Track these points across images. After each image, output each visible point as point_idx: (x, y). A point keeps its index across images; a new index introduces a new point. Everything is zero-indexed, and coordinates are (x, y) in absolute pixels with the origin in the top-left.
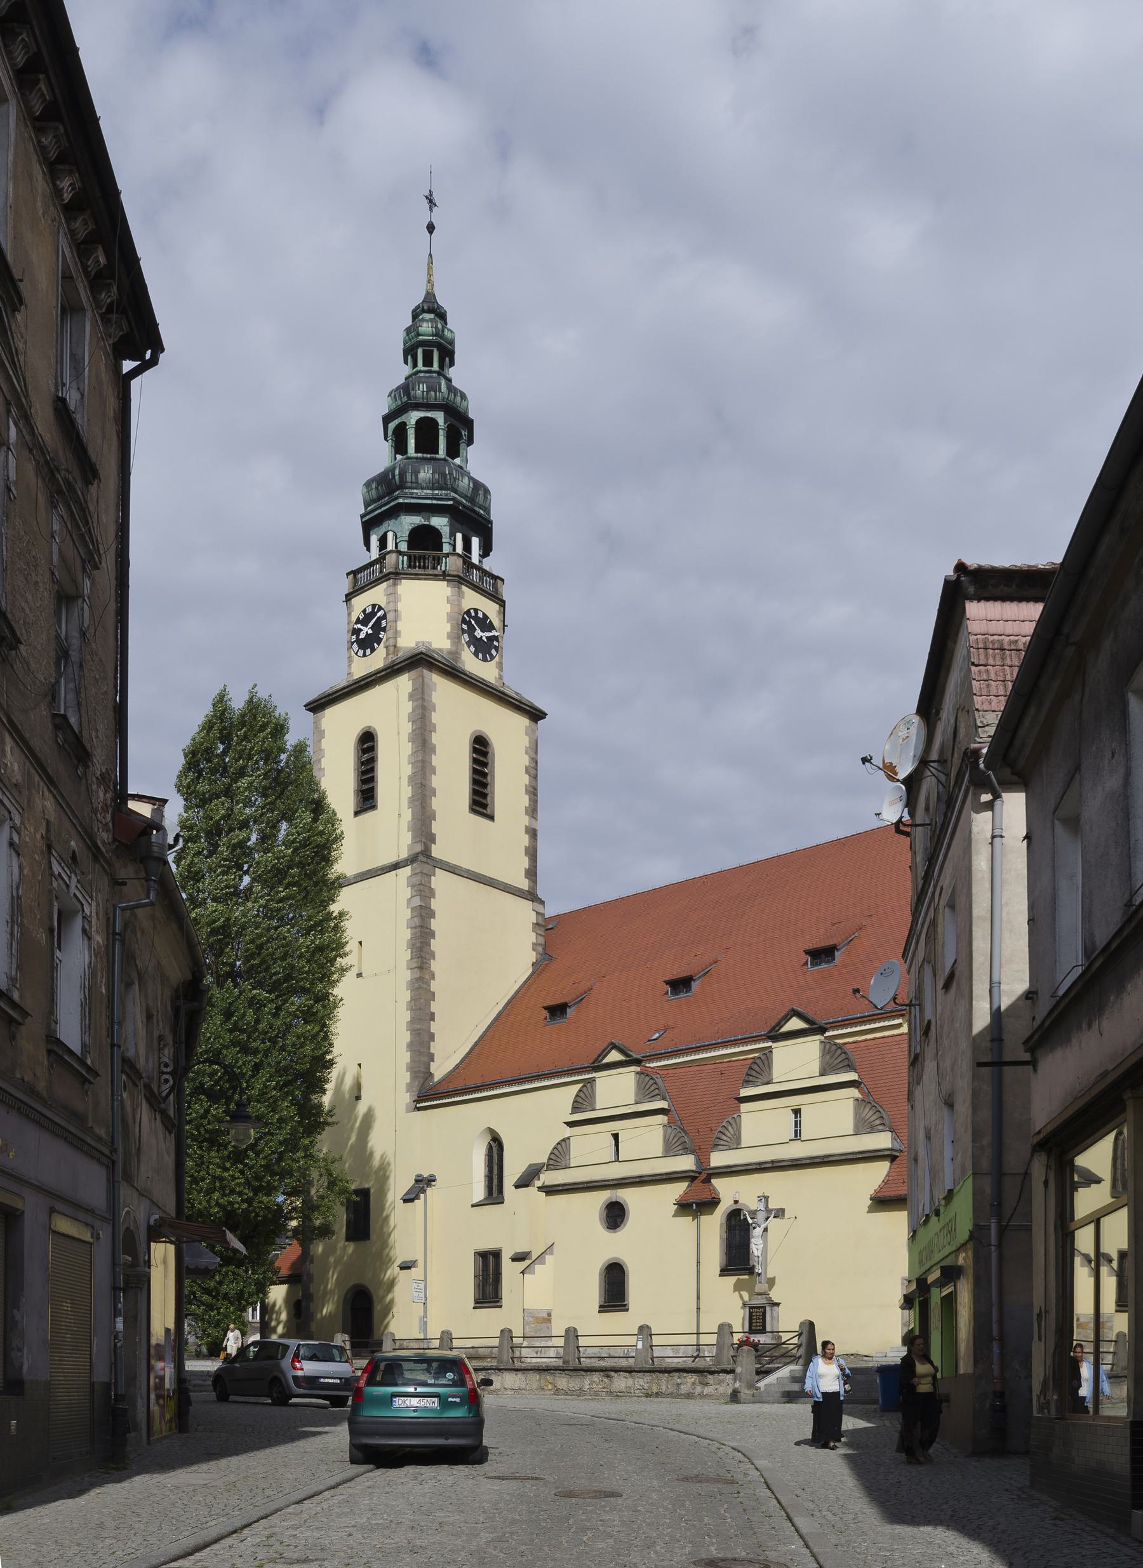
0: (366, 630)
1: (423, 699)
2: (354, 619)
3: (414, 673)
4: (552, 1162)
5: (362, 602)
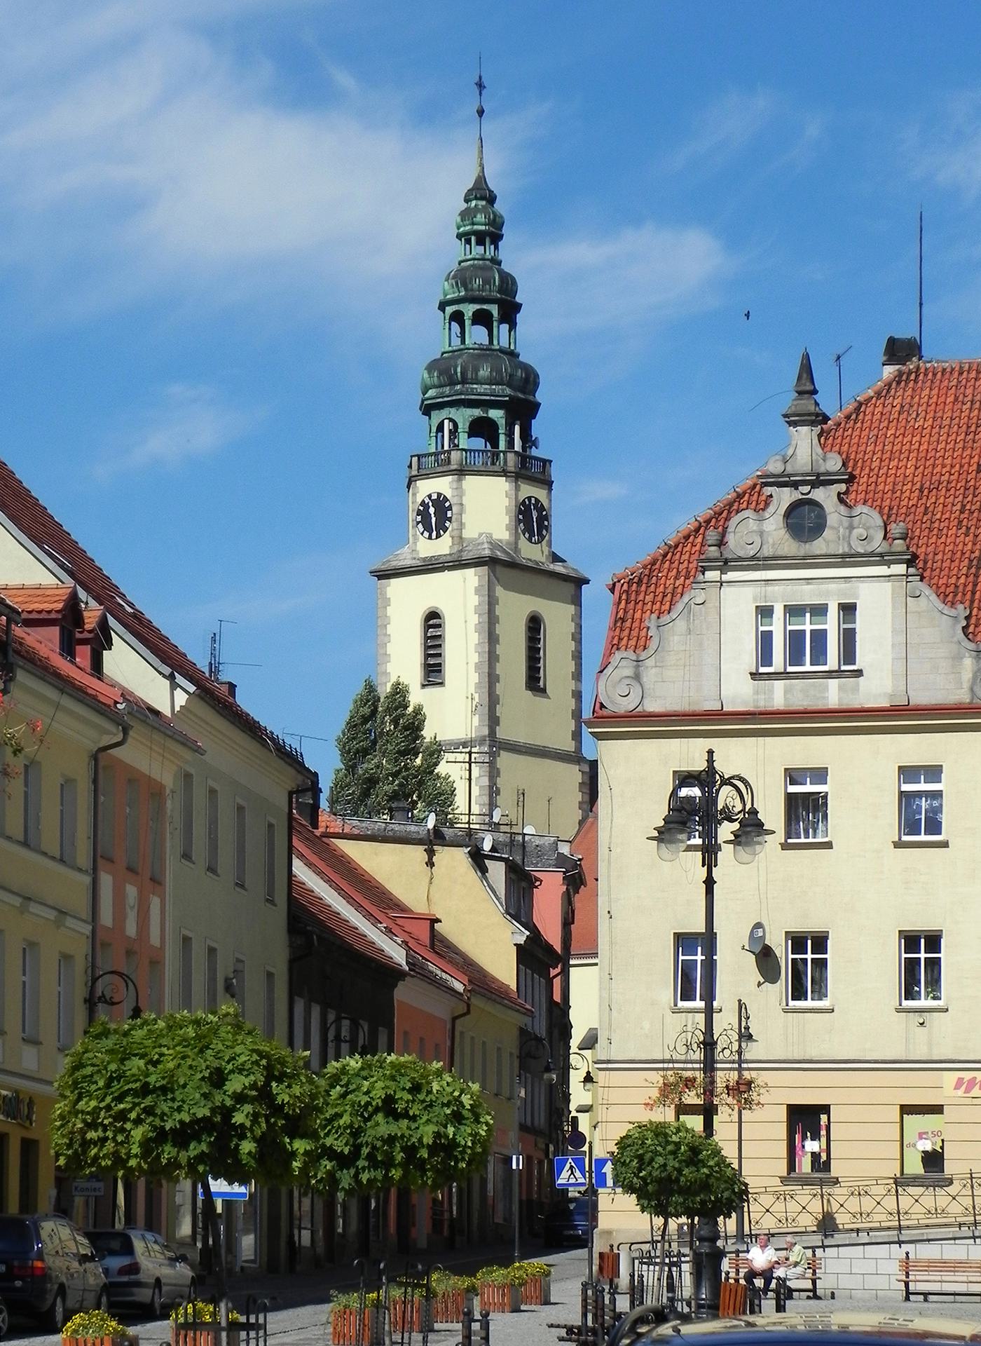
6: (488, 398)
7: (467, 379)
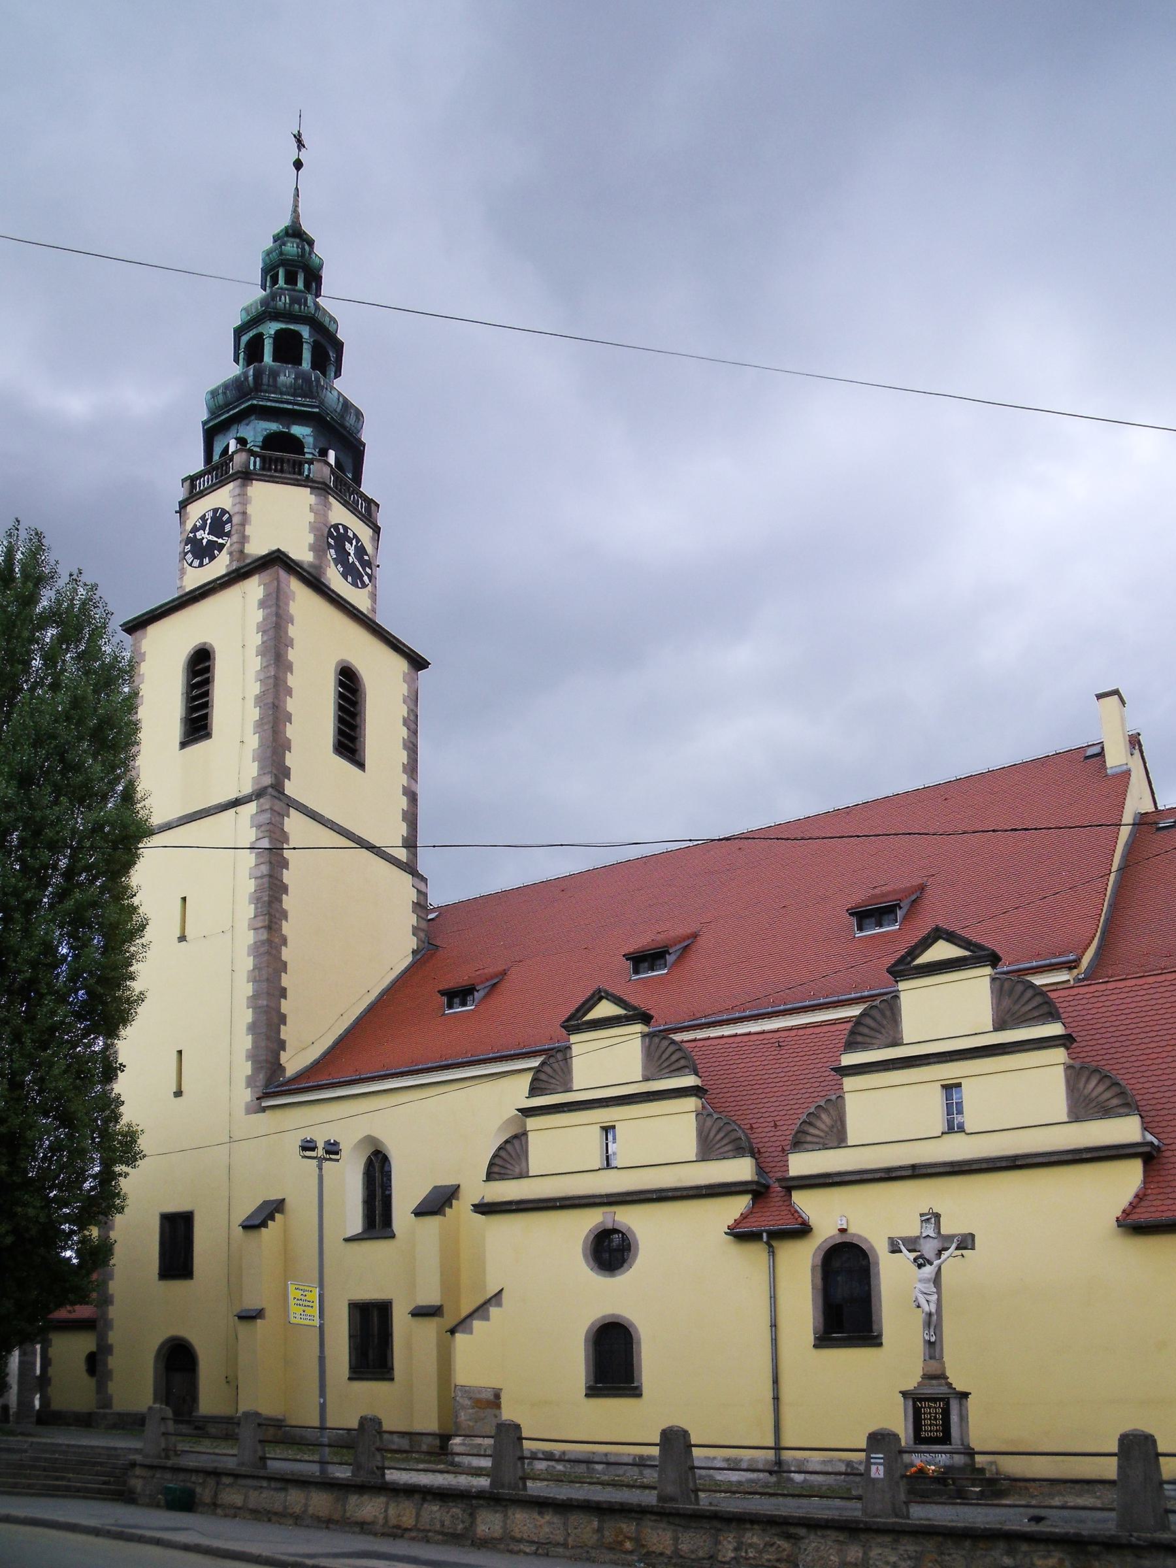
0: (205, 536)
1: (278, 606)
2: (189, 526)
3: (266, 576)
4: (496, 1169)
5: (199, 509)
6: (290, 407)
7: (262, 384)
